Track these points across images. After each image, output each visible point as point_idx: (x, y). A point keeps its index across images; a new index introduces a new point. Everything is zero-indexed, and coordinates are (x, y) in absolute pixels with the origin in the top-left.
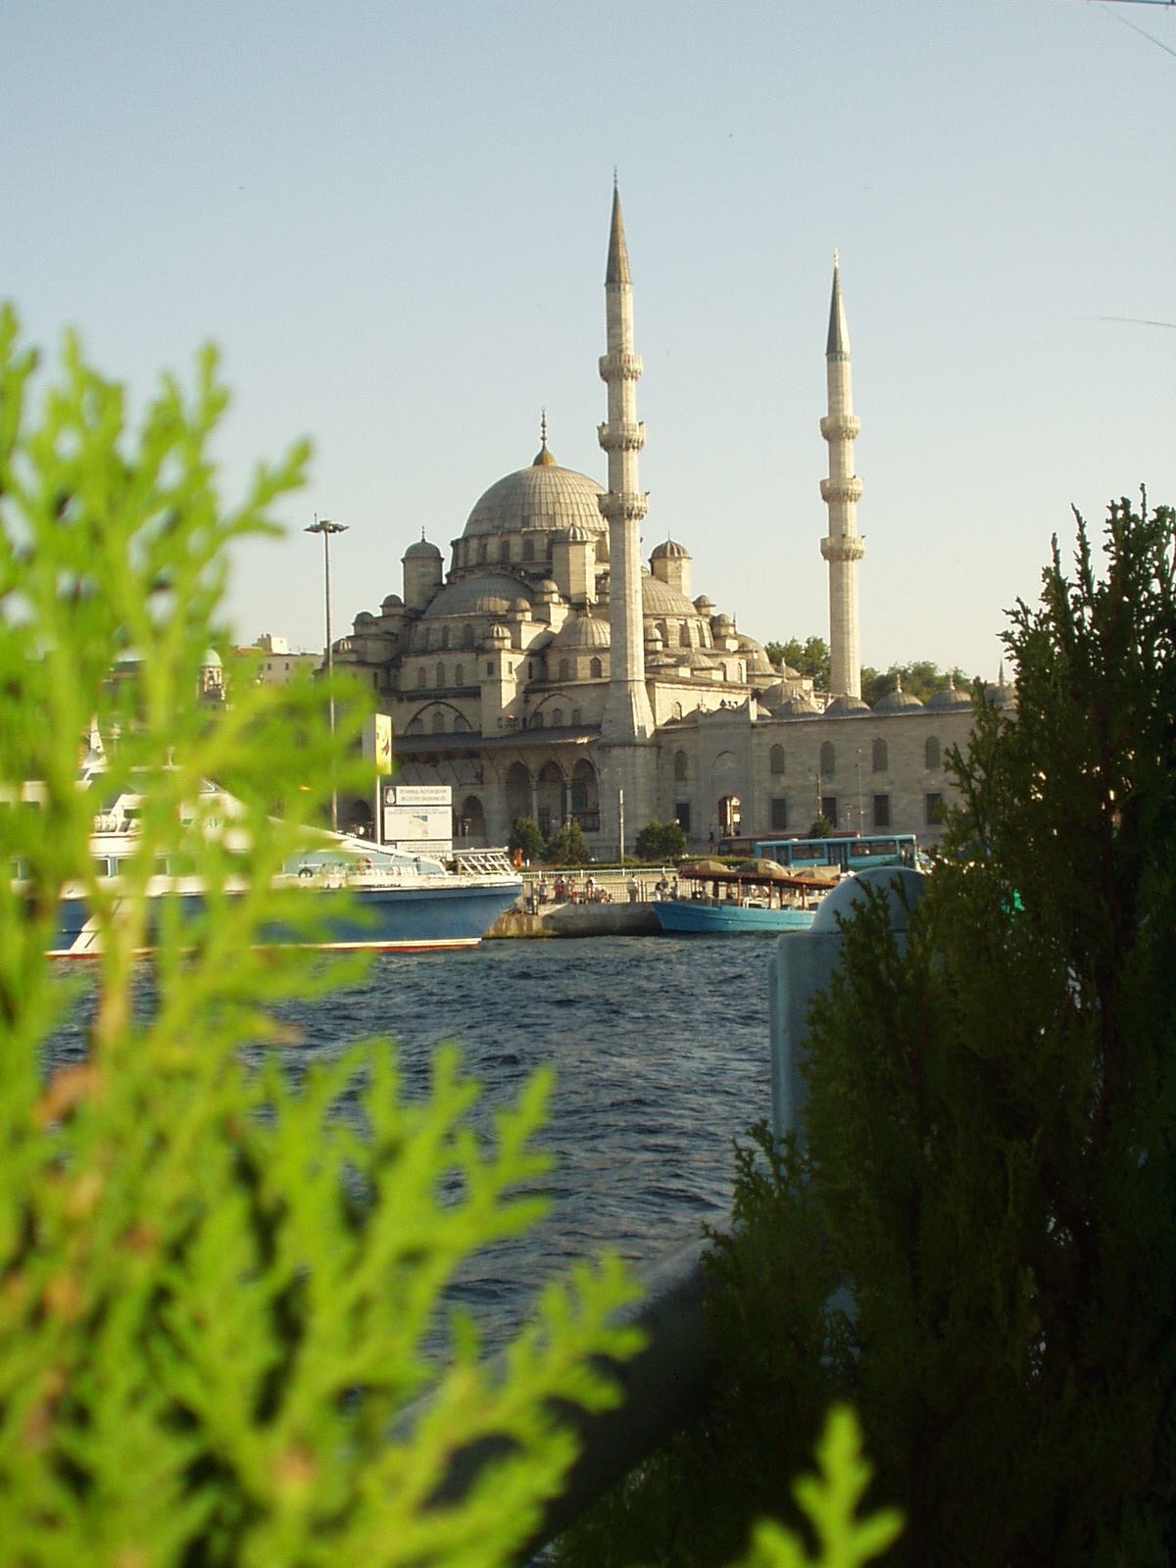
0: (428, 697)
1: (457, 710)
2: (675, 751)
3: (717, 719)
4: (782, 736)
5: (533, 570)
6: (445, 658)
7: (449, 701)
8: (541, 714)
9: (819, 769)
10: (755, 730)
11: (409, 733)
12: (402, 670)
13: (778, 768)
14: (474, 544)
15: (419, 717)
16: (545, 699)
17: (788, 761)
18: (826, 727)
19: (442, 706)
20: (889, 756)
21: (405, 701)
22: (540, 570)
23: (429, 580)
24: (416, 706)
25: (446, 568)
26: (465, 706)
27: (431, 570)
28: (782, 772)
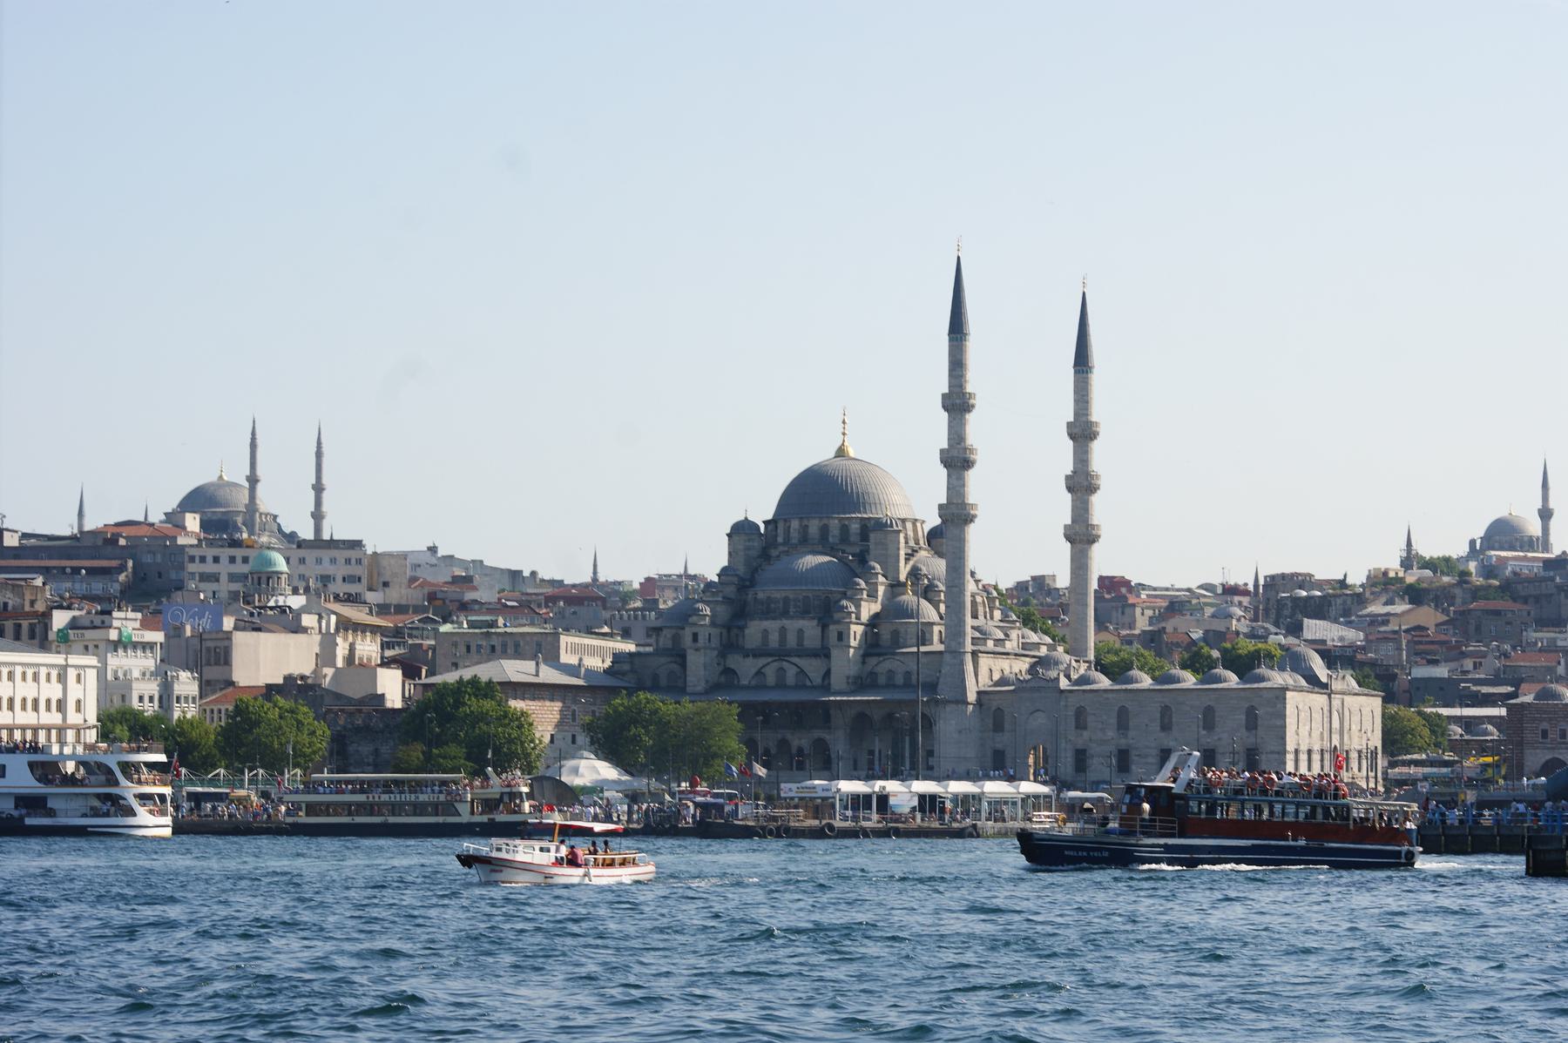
0: (770, 655)
2: (993, 709)
3: (1029, 685)
6: (786, 623)
8: (876, 674)
9: (1116, 727)
11: (753, 683)
12: (747, 631)
13: (1081, 725)
14: (795, 524)
16: (879, 662)
17: (1090, 719)
19: (784, 663)
20: (1174, 720)
21: (751, 657)
24: (762, 661)
27: (756, 544)
28: (1085, 728)
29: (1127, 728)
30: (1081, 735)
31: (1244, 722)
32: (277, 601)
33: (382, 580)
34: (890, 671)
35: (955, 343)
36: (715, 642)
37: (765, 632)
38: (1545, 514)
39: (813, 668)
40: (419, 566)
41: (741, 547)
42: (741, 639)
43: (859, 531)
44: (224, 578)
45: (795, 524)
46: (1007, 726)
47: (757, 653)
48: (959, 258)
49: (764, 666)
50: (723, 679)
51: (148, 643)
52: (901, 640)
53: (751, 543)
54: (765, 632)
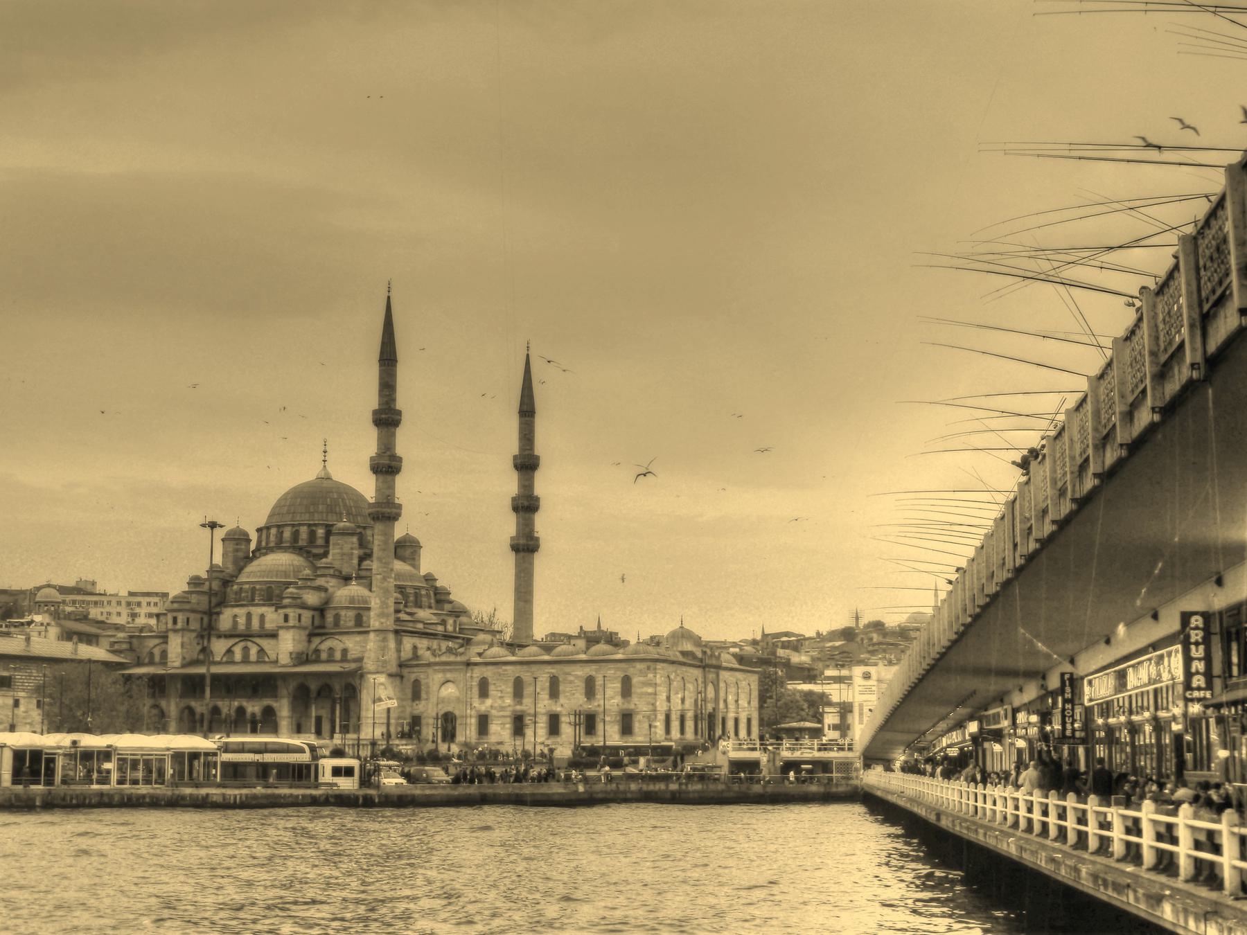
1: (258, 645)
2: (412, 680)
4: (488, 672)
5: (315, 551)
6: (251, 608)
10: (470, 668)
11: (225, 659)
12: (222, 617)
15: (232, 649)
17: (491, 688)
18: (519, 667)
19: (249, 644)
22: (321, 551)
23: (241, 554)
24: (231, 642)
25: (253, 546)
26: (266, 644)
27: (243, 547)
31: (620, 690)
34: (331, 649)
36: (195, 625)
41: (231, 549)
43: (323, 535)
46: (423, 695)
47: (228, 636)
49: (233, 645)
50: (201, 657)
52: (342, 622)
53: (239, 547)
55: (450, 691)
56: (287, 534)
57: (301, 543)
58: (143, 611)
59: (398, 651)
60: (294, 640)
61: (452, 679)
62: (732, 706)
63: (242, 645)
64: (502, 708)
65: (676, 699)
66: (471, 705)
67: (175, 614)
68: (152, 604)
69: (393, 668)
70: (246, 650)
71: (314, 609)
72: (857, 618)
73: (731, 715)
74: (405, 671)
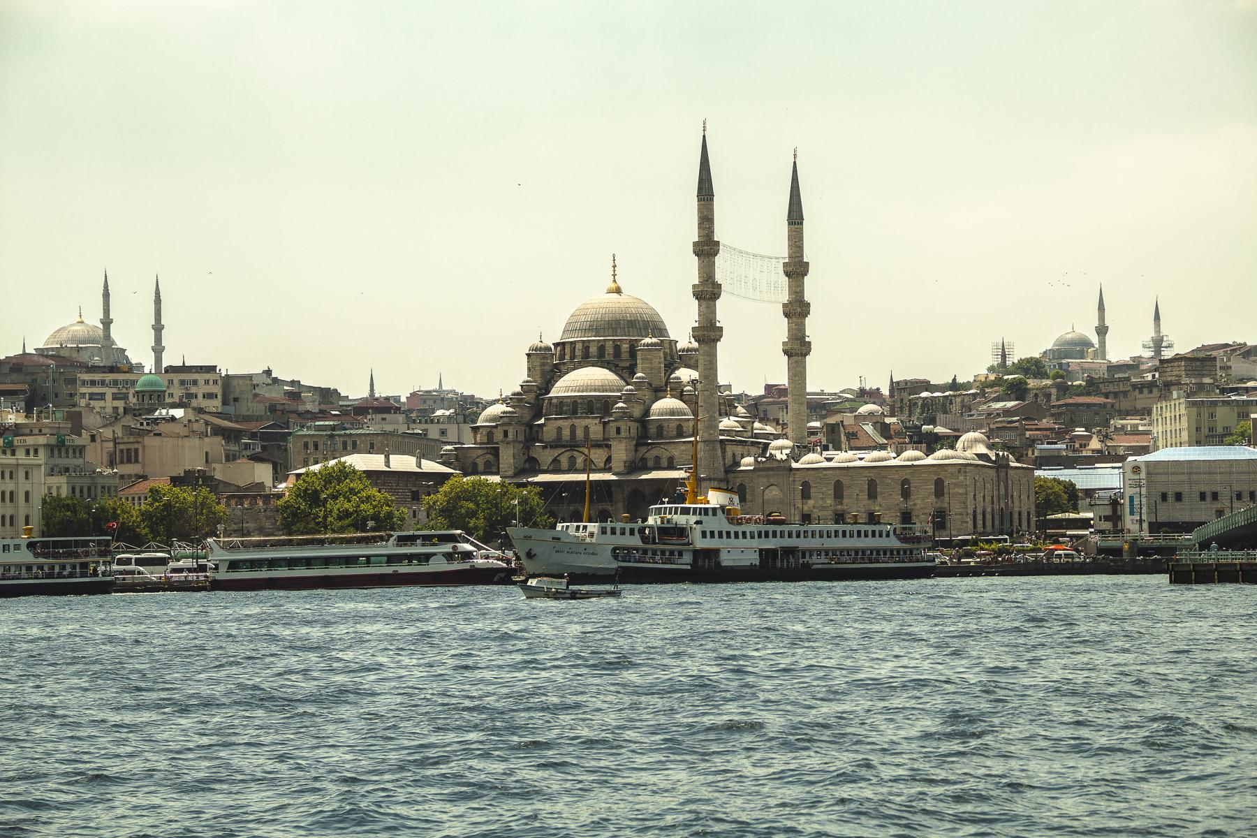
6: (576, 422)
7: (581, 449)
11: (551, 468)
20: (878, 490)
23: (548, 368)
24: (556, 452)
28: (809, 498)
29: (842, 498)
30: (806, 503)
32: (160, 414)
33: (232, 397)
35: (703, 202)
36: (521, 438)
37: (559, 429)
38: (1102, 330)
39: (598, 456)
40: (258, 385)
42: (540, 434)
44: (109, 397)
45: (579, 346)
48: (704, 136)
49: (559, 455)
50: (527, 466)
51: (77, 446)
54: (559, 429)
55: (774, 492)
56: (593, 350)
57: (607, 358)
58: (200, 390)
59: (724, 459)
60: (626, 450)
61: (775, 483)
62: (1017, 503)
63: (568, 454)
64: (823, 508)
65: (980, 498)
66: (794, 505)
67: (506, 428)
68: (211, 382)
69: (721, 475)
70: (572, 460)
71: (637, 421)
72: (1004, 356)
73: (1016, 509)
74: (731, 476)
